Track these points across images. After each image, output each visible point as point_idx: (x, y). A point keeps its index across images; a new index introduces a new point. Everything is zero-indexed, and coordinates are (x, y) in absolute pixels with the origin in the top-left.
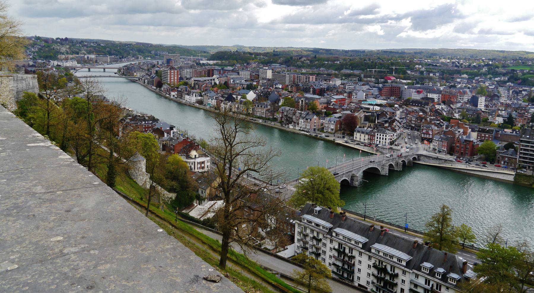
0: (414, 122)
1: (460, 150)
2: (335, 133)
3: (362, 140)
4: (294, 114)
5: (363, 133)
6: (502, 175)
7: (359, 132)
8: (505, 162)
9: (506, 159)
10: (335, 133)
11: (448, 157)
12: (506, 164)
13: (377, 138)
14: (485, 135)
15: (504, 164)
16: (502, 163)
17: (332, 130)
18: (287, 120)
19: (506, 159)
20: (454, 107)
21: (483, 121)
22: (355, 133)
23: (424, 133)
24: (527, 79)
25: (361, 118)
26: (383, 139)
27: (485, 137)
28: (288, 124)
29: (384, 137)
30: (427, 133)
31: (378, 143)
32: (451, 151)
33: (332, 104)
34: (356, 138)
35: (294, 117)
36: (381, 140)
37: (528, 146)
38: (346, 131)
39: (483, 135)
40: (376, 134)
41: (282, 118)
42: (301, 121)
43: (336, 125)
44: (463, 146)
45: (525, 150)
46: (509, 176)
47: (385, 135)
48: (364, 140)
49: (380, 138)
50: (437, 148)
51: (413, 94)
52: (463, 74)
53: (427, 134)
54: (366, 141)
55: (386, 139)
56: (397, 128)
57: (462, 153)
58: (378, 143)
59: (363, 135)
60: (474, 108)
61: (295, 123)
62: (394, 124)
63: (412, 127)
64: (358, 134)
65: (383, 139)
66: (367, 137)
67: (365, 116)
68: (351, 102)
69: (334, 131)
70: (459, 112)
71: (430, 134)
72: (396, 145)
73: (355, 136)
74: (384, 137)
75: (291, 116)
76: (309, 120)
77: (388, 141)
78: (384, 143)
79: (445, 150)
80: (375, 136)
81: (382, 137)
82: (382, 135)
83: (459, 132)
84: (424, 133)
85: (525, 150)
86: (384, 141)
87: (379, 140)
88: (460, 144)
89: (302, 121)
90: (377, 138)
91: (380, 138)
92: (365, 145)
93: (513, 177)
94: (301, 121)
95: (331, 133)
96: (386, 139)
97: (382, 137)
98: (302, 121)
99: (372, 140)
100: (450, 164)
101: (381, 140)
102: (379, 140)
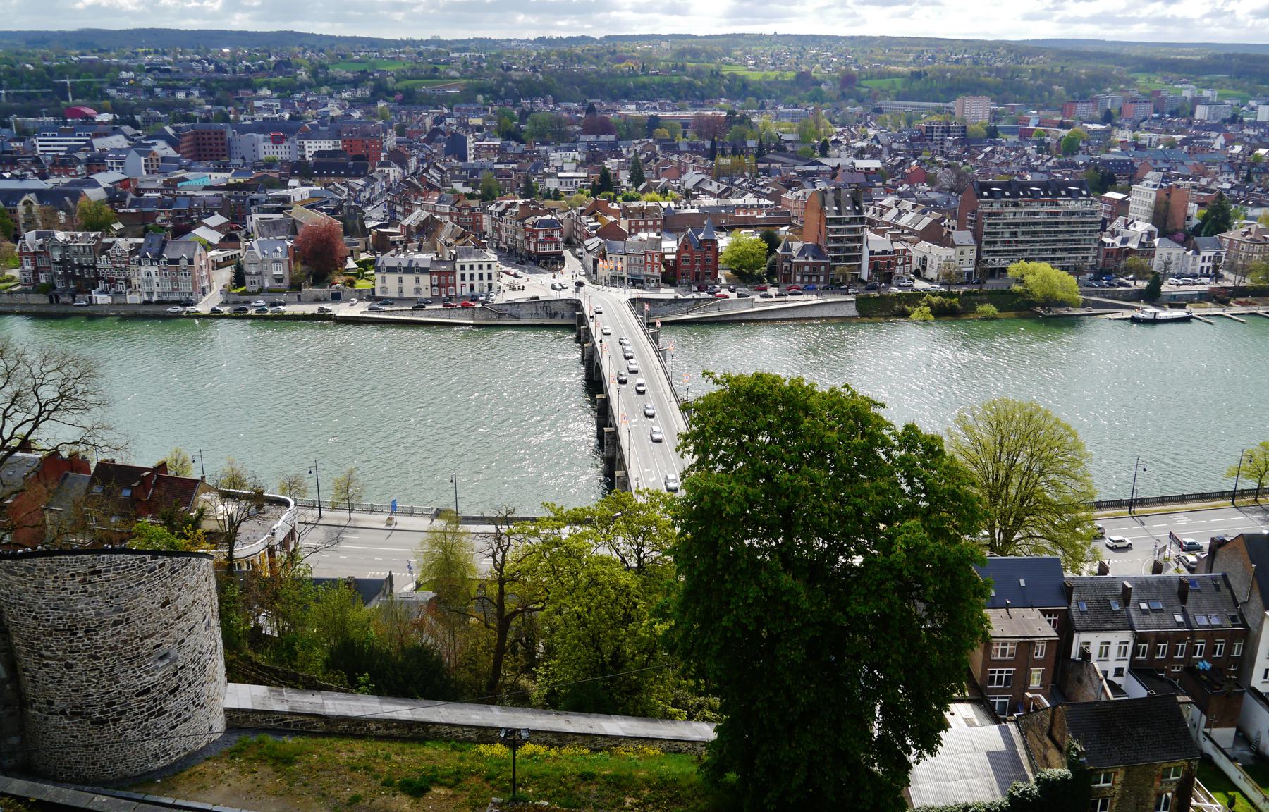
1: (693, 267)
6: (833, 307)
8: (803, 277)
9: (807, 268)
12: (806, 279)
13: (463, 277)
14: (646, 222)
15: (802, 281)
16: (798, 278)
17: (279, 280)
18: (68, 277)
23: (542, 242)
24: (413, 90)
26: (481, 276)
34: (384, 289)
35: (103, 263)
37: (841, 230)
44: (697, 256)
45: (837, 240)
46: (845, 307)
48: (418, 291)
49: (472, 276)
50: (624, 274)
52: (261, 87)
53: (551, 243)
57: (698, 274)
58: (466, 291)
59: (409, 279)
61: (111, 282)
65: (481, 276)
66: (425, 280)
71: (557, 242)
75: (86, 261)
76: (183, 263)
80: (454, 274)
85: (837, 240)
87: (468, 281)
88: (692, 253)
89: (153, 269)
90: (463, 277)
91: (472, 276)
93: (853, 306)
95: (281, 292)
99: (447, 285)
101: (476, 282)
102: (468, 281)
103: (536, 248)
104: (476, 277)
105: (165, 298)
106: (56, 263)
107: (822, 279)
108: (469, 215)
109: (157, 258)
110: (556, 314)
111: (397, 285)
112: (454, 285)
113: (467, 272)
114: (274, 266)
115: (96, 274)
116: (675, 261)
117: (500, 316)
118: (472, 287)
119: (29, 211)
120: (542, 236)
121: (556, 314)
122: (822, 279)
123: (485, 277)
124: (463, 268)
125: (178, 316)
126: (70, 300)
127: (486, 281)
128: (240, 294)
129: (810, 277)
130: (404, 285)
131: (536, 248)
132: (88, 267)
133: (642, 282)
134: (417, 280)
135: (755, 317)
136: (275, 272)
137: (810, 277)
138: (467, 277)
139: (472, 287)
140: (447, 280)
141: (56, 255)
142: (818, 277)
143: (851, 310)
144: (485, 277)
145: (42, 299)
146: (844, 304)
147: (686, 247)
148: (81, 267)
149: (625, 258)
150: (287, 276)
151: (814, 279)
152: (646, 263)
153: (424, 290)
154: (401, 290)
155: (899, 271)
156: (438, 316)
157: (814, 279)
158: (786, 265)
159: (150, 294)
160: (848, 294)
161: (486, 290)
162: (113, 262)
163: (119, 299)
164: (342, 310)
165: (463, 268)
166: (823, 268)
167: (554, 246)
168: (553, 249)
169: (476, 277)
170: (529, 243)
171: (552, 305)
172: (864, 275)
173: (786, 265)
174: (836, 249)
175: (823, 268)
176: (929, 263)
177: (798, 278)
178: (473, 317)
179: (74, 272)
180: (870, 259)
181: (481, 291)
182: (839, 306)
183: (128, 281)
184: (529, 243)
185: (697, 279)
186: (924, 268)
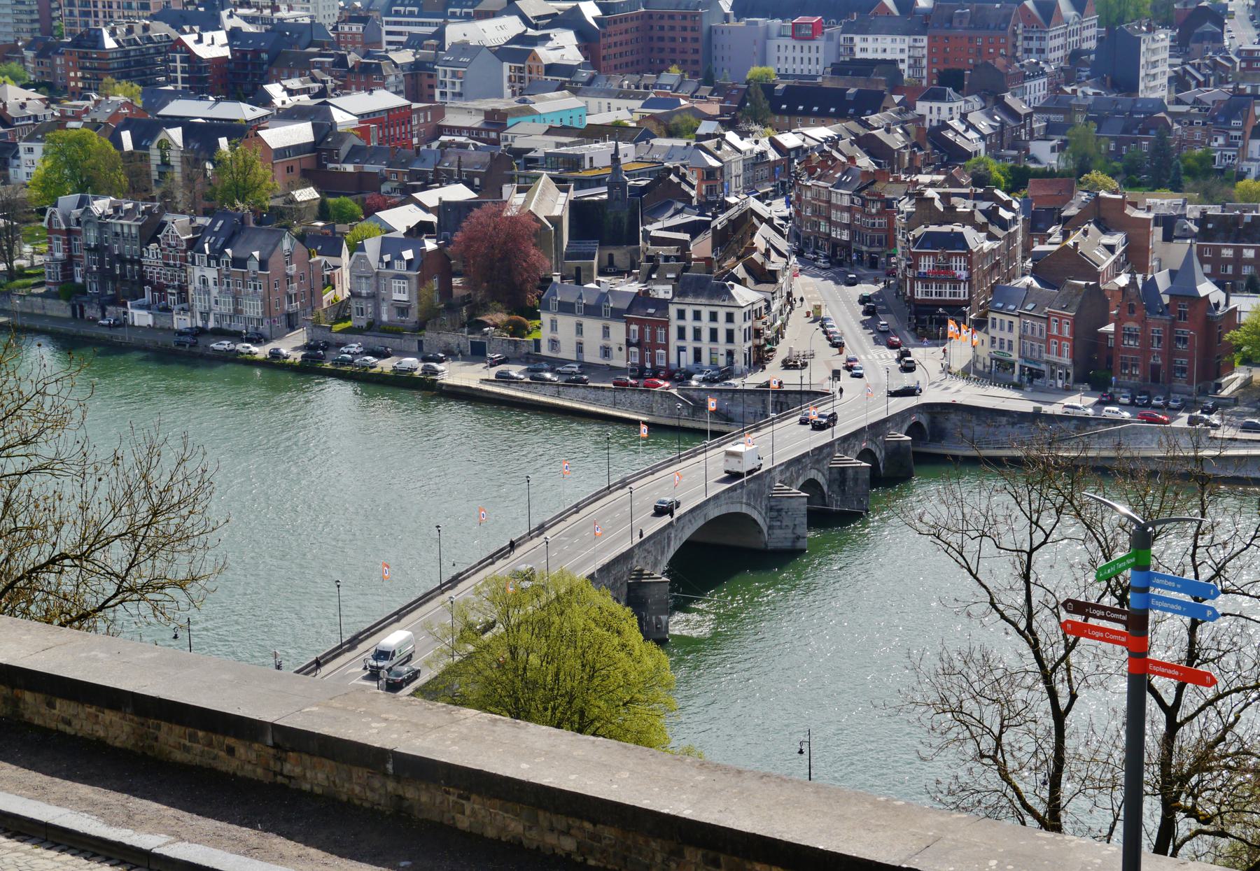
0: (846, 218)
1: (1145, 350)
2: (421, 326)
3: (592, 356)
4: (152, 230)
5: (593, 311)
7: (566, 308)
10: (421, 326)
11: (1082, 402)
13: (681, 333)
14: (1238, 251)
17: (403, 310)
18: (105, 276)
20: (1023, 109)
21: (1190, 172)
22: (545, 317)
23: (924, 278)
25: (556, 221)
26: (714, 335)
27: (1238, 260)
28: (115, 301)
29: (722, 326)
30: (943, 274)
31: (687, 359)
32: (1094, 368)
33: (344, 149)
34: (554, 343)
36: (705, 344)
38: (484, 307)
39: (1228, 253)
40: (673, 311)
41: (68, 265)
42: (202, 273)
43: (422, 281)
48: (606, 352)
49: (697, 334)
50: (1015, 356)
51: (772, 44)
54: (619, 360)
55: (730, 336)
56: (776, 263)
57: (1155, 370)
58: (687, 359)
59: (593, 327)
60: (1123, 100)
61: (160, 289)
62: (759, 242)
63: (836, 244)
64: (567, 323)
65: (714, 335)
66: (618, 331)
67: (576, 208)
68: (441, 130)
69: (413, 317)
70: (1051, 130)
71: (956, 281)
72: (787, 365)
73: (544, 335)
74: (722, 326)
75: (130, 249)
77: (742, 347)
78: (722, 362)
79: (1066, 360)
80: (666, 325)
81: (705, 325)
83: (1111, 249)
84: (924, 278)
86: (722, 346)
87: (690, 343)
88: (1143, 322)
89: (211, 274)
90: (681, 333)
91: (697, 334)
92: (622, 386)
94: (202, 273)
96: (730, 336)
98: (211, 274)
99: (654, 346)
101: (705, 344)
102: (690, 343)
104: (706, 335)
105: (225, 325)
106: (89, 250)
108: (879, 214)
109: (217, 255)
111: (575, 338)
112: (666, 347)
113: (689, 323)
114: (396, 284)
115: (142, 274)
118: (697, 352)
119: (165, 164)
120: (926, 264)
123: (722, 336)
124: (681, 314)
125: (231, 358)
126: (99, 315)
127: (722, 346)
128: (343, 331)
130: (585, 339)
132: (132, 262)
134: (606, 332)
136: (396, 296)
138: (689, 334)
139: (697, 352)
140: (654, 335)
141: (92, 237)
144: (722, 336)
145: (60, 309)
148: (121, 259)
149: (1016, 321)
150: (415, 303)
152: (1049, 337)
153: (615, 351)
154: (580, 348)
156: (595, 402)
159: (205, 316)
162: (166, 257)
163: (163, 321)
164: (455, 374)
165: (681, 314)
167: (947, 289)
169: (706, 335)
179: (113, 268)
183: (182, 290)
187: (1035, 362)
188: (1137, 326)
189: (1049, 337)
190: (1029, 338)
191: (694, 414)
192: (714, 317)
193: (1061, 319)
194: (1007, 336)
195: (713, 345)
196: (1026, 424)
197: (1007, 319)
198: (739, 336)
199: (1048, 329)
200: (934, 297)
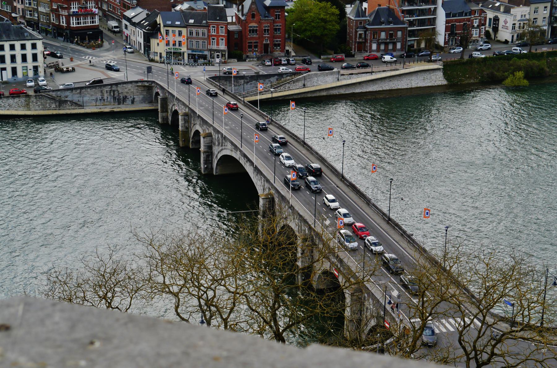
1: (261, 38)
6: (420, 77)
9: (383, 35)
16: (374, 47)
19: (383, 35)
23: (75, 14)
44: (266, 25)
47: (28, 44)
49: (13, 58)
50: (184, 49)
53: (85, 16)
57: (266, 46)
71: (93, 15)
74: (29, 52)
82: (18, 44)
88: (259, 22)
91: (13, 58)
93: (440, 74)
97: (18, 52)
100: (300, 84)
103: (68, 22)
104: (19, 59)
107: (399, 46)
110: (125, 98)
116: (240, 33)
117: (61, 103)
118: (14, 71)
121: (125, 98)
122: (399, 46)
123: (29, 58)
129: (386, 44)
131: (68, 22)
133: (205, 57)
135: (342, 91)
137: (386, 44)
139: (14, 71)
142: (395, 44)
143: (439, 79)
144: (29, 58)
146: (426, 74)
147: (253, 16)
149: (184, 31)
151: (390, 47)
155: (475, 34)
157: (390, 47)
158: (361, 32)
160: (430, 61)
161: (31, 74)
166: (399, 34)
168: (88, 22)
169: (19, 59)
170: (58, 17)
171: (120, 88)
172: (441, 39)
173: (361, 32)
174: (410, 13)
175: (399, 34)
176: (501, 23)
177: (374, 47)
178: (27, 106)
180: (447, 22)
181: (26, 75)
182: (426, 75)
184: (58, 17)
185: (266, 51)
186: (496, 30)
187: (201, 51)
188: (256, 25)
189: (209, 36)
190: (194, 38)
191: (59, 106)
192: (23, 47)
193: (218, 25)
194: (178, 39)
195: (24, 64)
196: (254, 82)
197: (177, 30)
198: (40, 57)
199: (209, 31)
200: (82, 25)
